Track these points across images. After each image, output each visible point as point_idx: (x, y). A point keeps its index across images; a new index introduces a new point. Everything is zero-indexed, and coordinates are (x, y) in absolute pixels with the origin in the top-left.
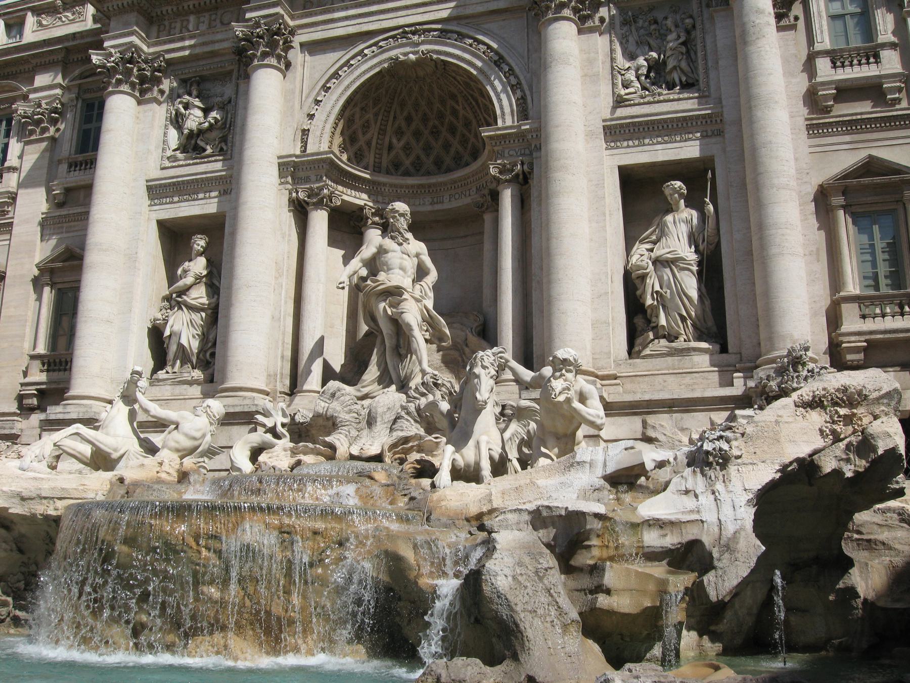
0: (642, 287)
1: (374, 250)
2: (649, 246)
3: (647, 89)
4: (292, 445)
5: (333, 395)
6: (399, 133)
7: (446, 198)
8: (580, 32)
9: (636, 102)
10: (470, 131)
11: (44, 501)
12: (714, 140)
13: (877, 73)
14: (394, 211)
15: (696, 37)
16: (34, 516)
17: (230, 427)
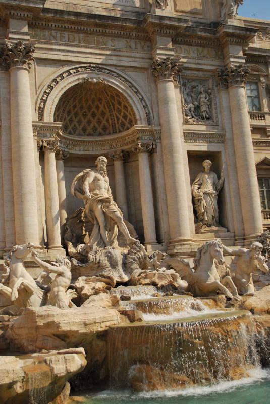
0: (199, 204)
1: (93, 179)
2: (197, 186)
3: (194, 118)
4: (84, 278)
5: (96, 252)
6: (69, 112)
7: (91, 149)
8: (175, 87)
9: (192, 122)
10: (103, 118)
11: (97, 324)
12: (221, 145)
13: (265, 124)
14: (103, 161)
15: (211, 98)
16: (91, 332)
17: (34, 269)
